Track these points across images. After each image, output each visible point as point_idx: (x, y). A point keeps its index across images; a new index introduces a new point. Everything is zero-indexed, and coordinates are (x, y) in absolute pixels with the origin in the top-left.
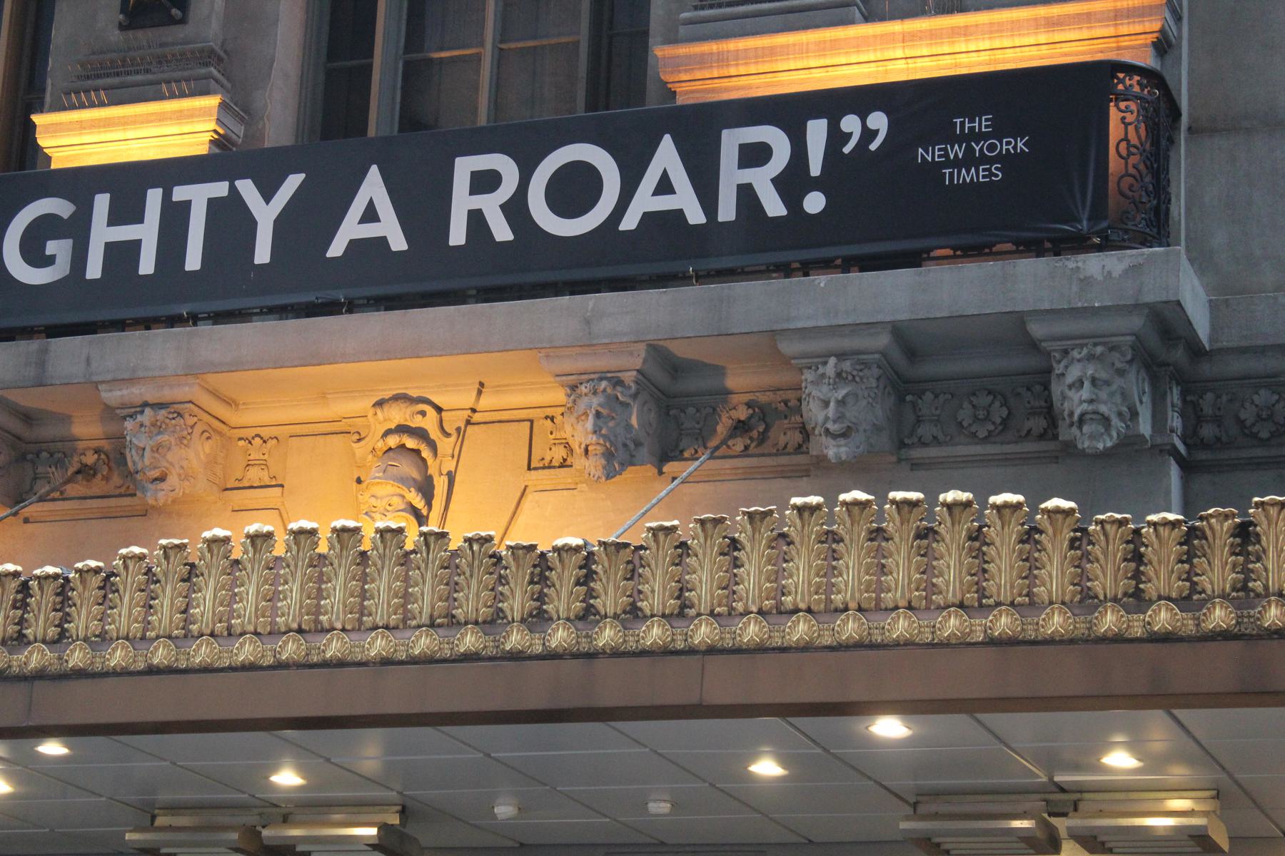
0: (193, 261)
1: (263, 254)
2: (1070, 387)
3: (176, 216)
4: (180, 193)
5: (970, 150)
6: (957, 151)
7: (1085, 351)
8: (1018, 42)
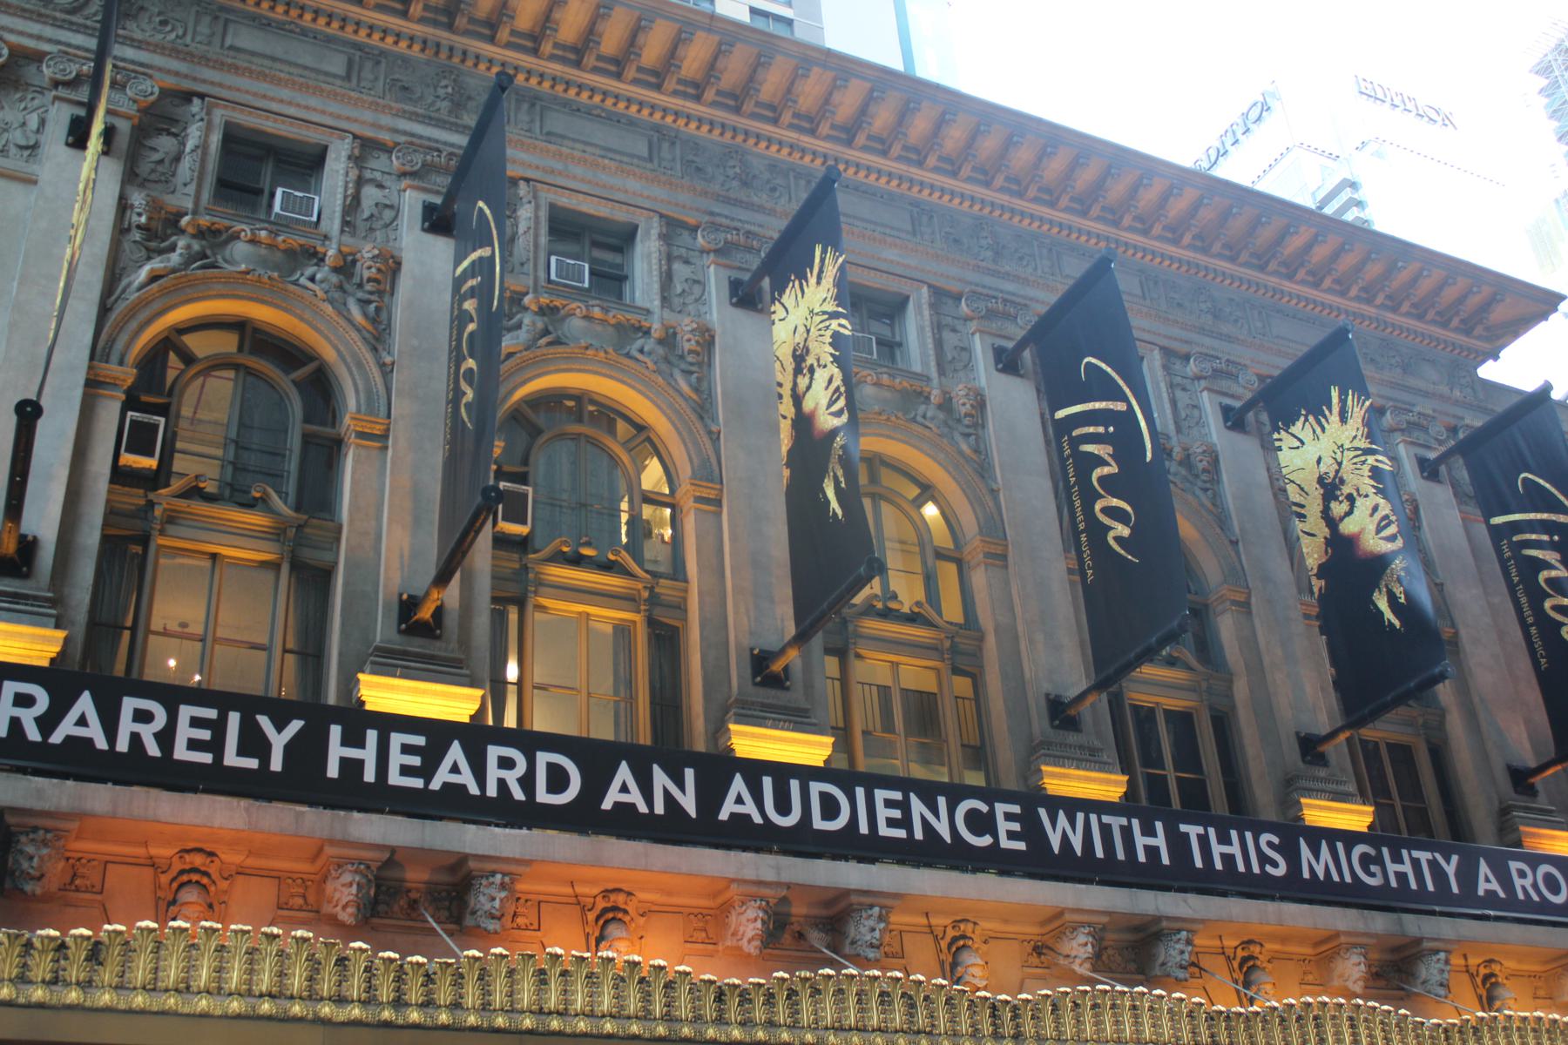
0: (1431, 887)
1: (1455, 890)
3: (1416, 863)
4: (1415, 854)
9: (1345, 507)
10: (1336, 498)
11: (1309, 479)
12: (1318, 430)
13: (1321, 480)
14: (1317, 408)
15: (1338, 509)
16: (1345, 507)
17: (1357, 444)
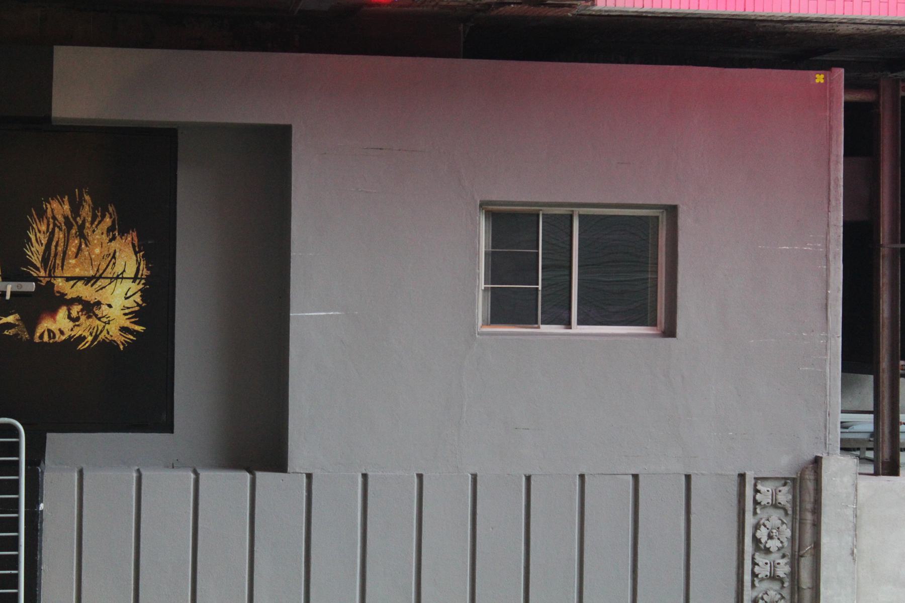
9: (74, 314)
10: (82, 310)
11: (104, 296)
12: (127, 311)
13: (98, 304)
14: (138, 315)
15: (76, 309)
16: (74, 314)
17: (105, 332)
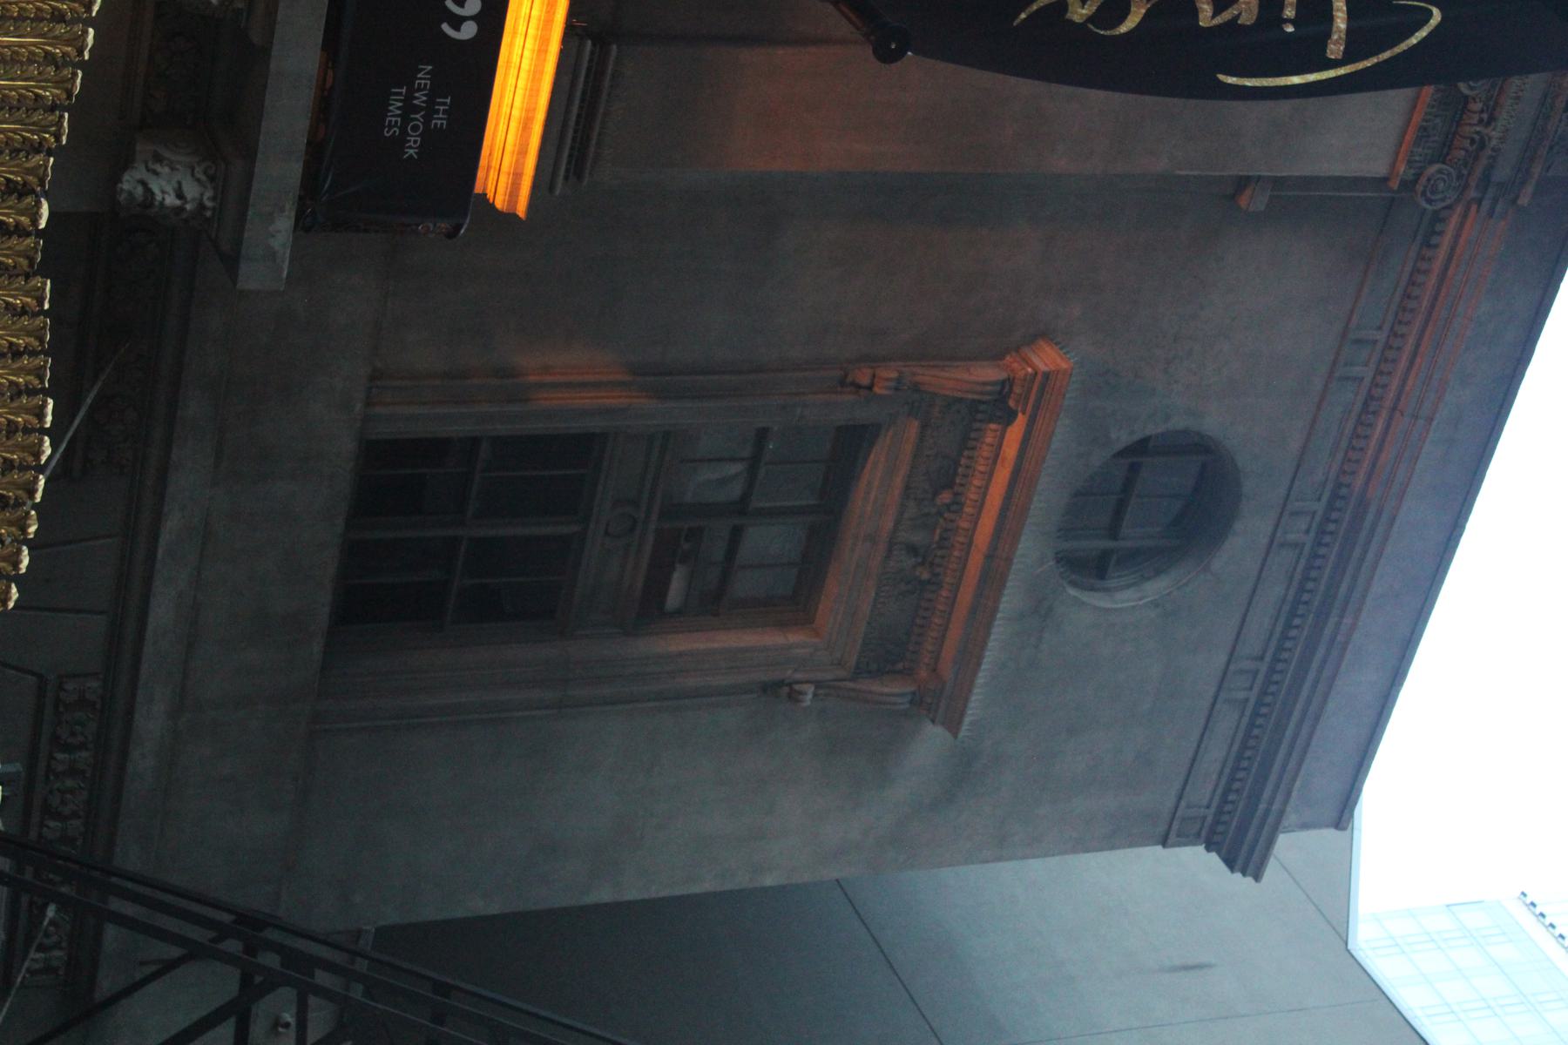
2: (179, 183)
5: (417, 109)
6: (420, 99)
7: (209, 204)
8: (520, 92)
